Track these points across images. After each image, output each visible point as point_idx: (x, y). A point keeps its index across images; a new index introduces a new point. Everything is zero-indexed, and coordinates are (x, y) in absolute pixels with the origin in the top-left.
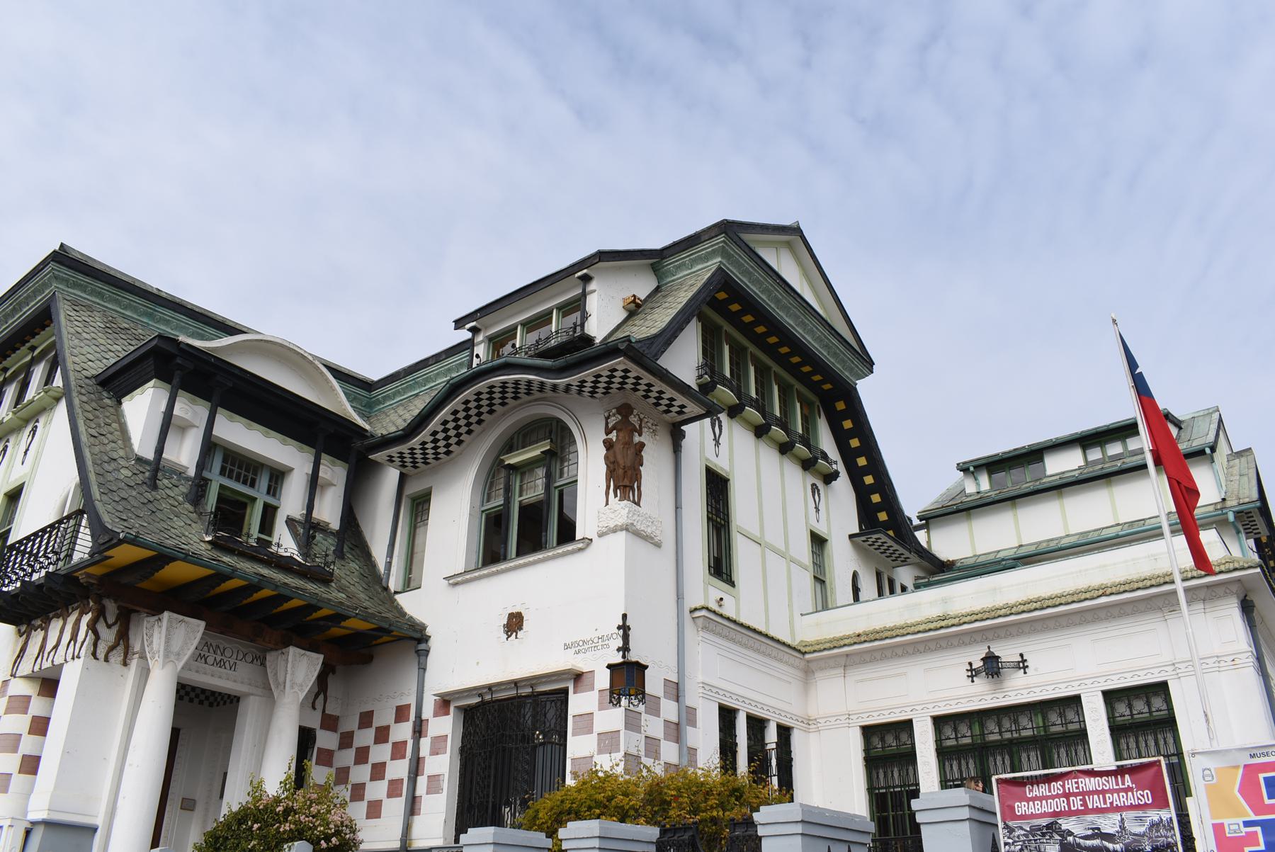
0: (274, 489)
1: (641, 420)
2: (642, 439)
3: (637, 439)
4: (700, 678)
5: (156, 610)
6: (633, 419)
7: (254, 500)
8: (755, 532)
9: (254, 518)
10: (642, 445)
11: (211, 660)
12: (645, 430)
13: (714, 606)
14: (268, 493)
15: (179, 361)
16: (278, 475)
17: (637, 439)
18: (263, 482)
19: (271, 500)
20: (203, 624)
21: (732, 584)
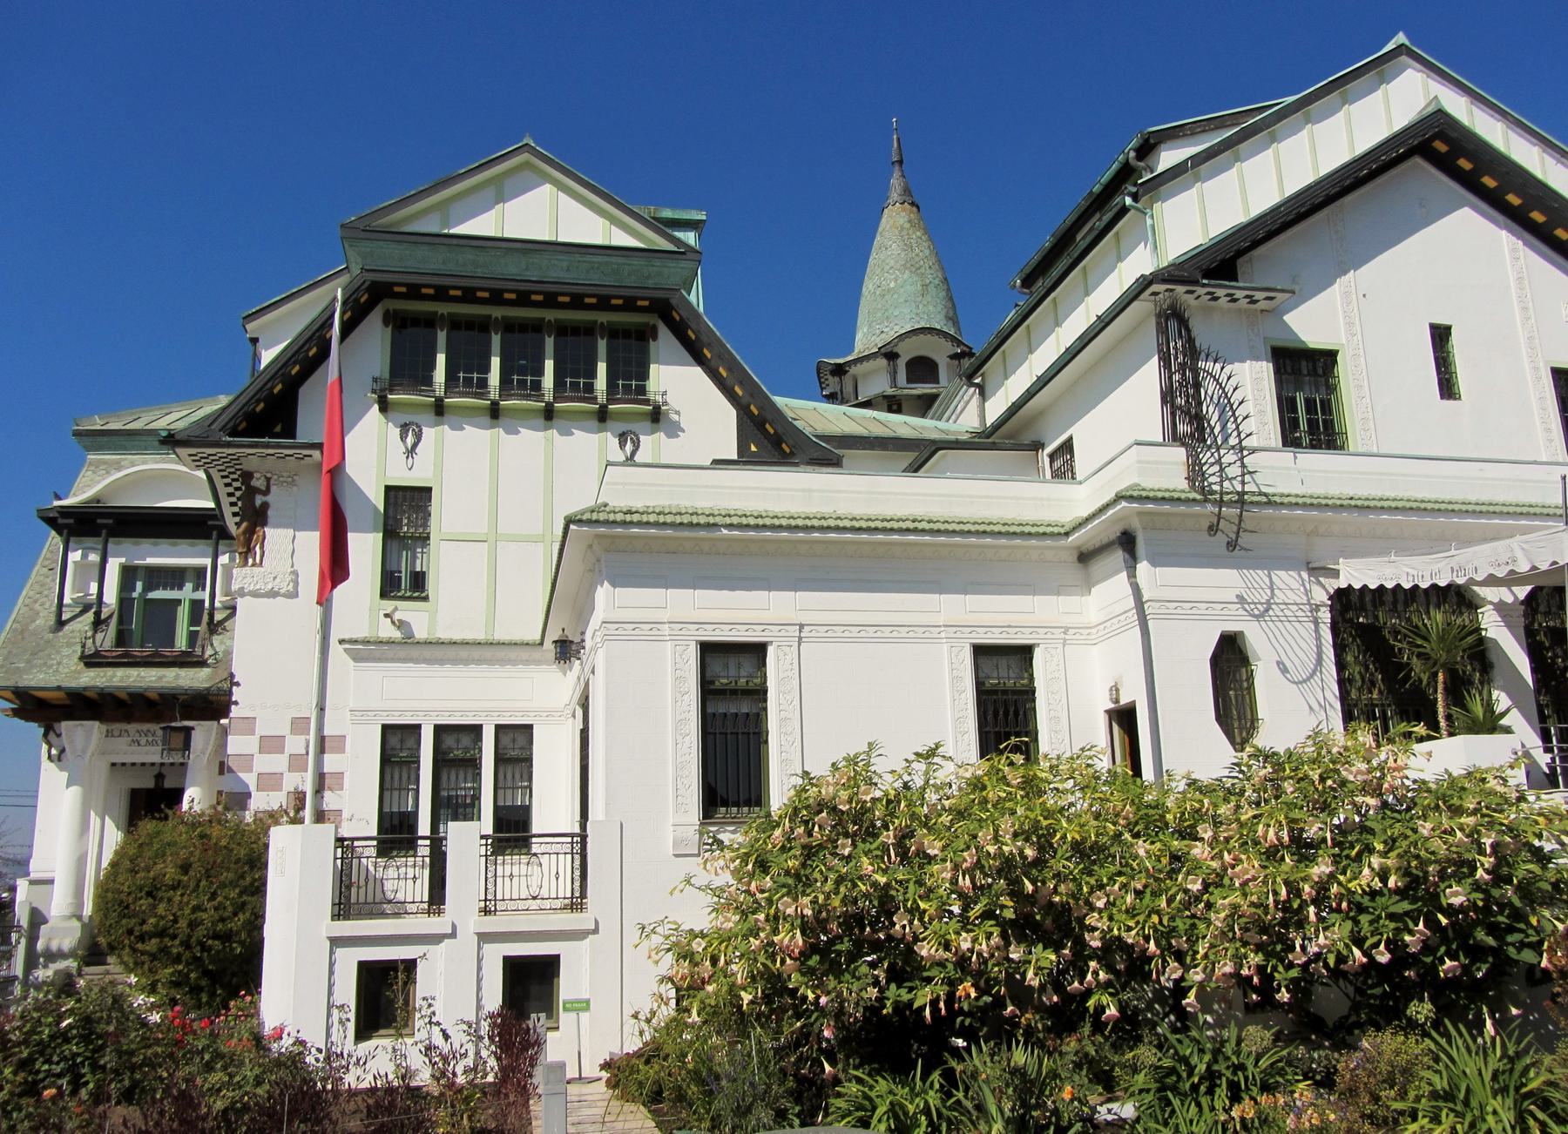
0: (200, 585)
1: (268, 480)
2: (269, 499)
3: (259, 500)
4: (351, 706)
5: (59, 721)
6: (258, 482)
7: (179, 602)
8: (482, 528)
9: (183, 614)
10: (265, 505)
11: (143, 741)
12: (273, 488)
13: (388, 631)
14: (195, 589)
15: (60, 521)
16: (200, 573)
17: (259, 500)
18: (189, 586)
19: (198, 595)
20: (97, 724)
21: (426, 599)
